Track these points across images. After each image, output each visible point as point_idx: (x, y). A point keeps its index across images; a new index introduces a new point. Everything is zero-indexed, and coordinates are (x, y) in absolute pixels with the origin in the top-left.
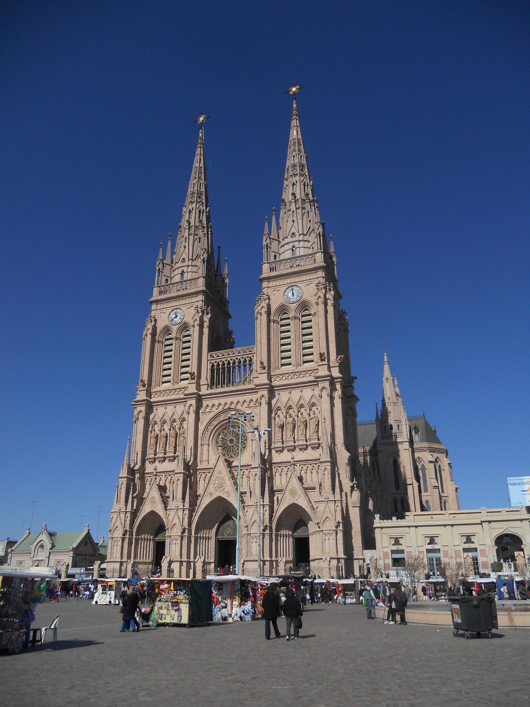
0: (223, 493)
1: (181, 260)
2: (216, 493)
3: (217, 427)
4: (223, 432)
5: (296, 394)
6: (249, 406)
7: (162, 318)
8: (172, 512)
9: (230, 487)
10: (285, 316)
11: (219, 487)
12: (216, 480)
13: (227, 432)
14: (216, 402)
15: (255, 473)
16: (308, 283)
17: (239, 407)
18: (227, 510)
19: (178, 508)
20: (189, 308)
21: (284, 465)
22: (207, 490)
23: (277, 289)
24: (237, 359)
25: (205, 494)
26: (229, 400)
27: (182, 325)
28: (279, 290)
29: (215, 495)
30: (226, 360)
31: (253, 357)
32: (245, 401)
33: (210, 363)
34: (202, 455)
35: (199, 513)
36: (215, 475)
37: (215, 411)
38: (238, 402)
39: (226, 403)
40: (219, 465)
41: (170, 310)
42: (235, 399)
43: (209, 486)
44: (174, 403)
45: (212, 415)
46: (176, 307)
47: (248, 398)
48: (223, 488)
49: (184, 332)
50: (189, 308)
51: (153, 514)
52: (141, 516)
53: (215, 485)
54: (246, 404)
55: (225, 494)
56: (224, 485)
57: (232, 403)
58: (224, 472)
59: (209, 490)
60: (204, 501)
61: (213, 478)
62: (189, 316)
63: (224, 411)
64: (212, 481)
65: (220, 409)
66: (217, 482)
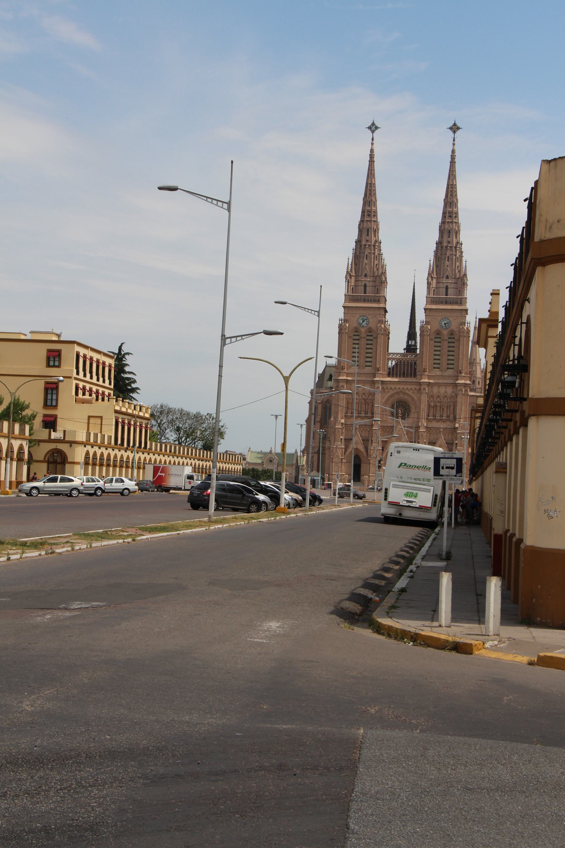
5: (442, 390)
10: (438, 336)
14: (393, 387)
16: (455, 318)
17: (407, 392)
21: (433, 429)
23: (435, 318)
24: (406, 360)
26: (401, 387)
30: (399, 360)
31: (417, 360)
32: (411, 389)
37: (392, 392)
38: (407, 389)
39: (399, 388)
42: (405, 387)
45: (389, 394)
46: (363, 315)
47: (414, 387)
50: (373, 317)
51: (357, 450)
52: (349, 450)
54: (411, 391)
57: (403, 388)
63: (397, 393)
65: (395, 391)
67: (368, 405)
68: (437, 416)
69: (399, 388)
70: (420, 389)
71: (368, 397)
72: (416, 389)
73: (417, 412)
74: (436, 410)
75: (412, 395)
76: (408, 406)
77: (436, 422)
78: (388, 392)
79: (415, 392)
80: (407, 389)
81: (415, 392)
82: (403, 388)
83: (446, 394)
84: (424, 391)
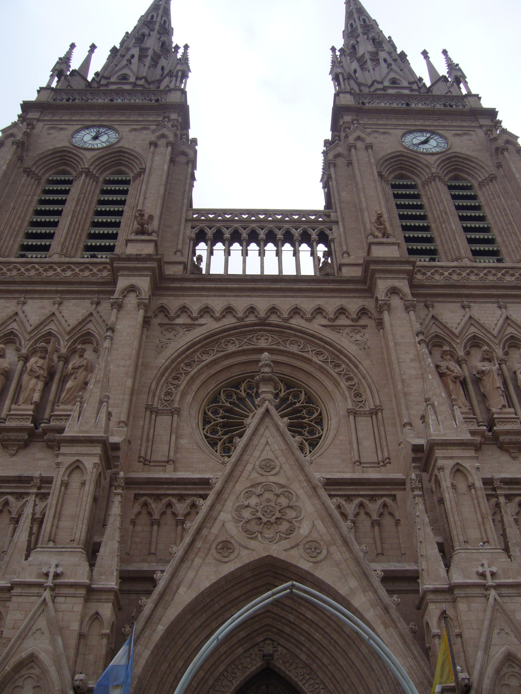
0: (286, 544)
1: (119, 74)
2: (253, 544)
3: (212, 371)
4: (229, 396)
6: (334, 324)
7: (51, 136)
8: (20, 599)
9: (319, 524)
11: (264, 520)
12: (248, 494)
13: (243, 394)
15: (450, 463)
17: (297, 322)
18: (269, 649)
19: (58, 581)
20: (135, 130)
22: (205, 532)
25: (199, 544)
27: (111, 153)
28: (384, 133)
29: (245, 552)
31: (331, 230)
32: (319, 311)
33: (193, 228)
34: (150, 444)
35: (161, 629)
36: (245, 474)
38: (296, 311)
39: (252, 310)
40: (263, 441)
41: (80, 126)
43: (214, 513)
44: (57, 292)
45: (196, 334)
48: (284, 526)
49: (112, 174)
50: (135, 130)
53: (247, 514)
54: (320, 320)
55: (294, 552)
56: (291, 514)
57: (273, 310)
58: (286, 467)
59: (215, 530)
60: (191, 574)
61: (241, 486)
62: (134, 140)
64: (233, 498)
65: (229, 321)
66: (253, 501)
67: (64, 380)
68: (504, 421)
69: (252, 310)
70: (363, 312)
71: (73, 351)
72: (342, 311)
73: (374, 412)
74: (484, 397)
75: (328, 334)
76: (309, 399)
77: (505, 458)
78: (189, 327)
79: (339, 322)
80: (296, 311)
81: (339, 322)
82: (273, 310)
83: (510, 330)
84: (396, 302)
